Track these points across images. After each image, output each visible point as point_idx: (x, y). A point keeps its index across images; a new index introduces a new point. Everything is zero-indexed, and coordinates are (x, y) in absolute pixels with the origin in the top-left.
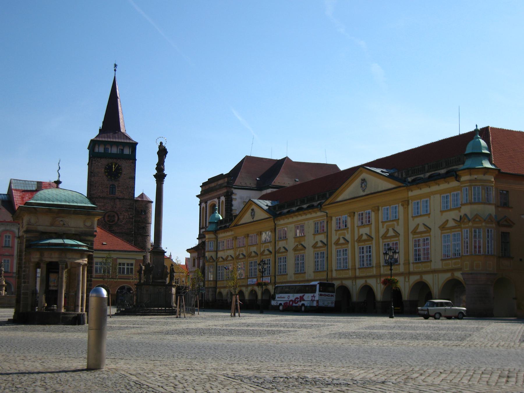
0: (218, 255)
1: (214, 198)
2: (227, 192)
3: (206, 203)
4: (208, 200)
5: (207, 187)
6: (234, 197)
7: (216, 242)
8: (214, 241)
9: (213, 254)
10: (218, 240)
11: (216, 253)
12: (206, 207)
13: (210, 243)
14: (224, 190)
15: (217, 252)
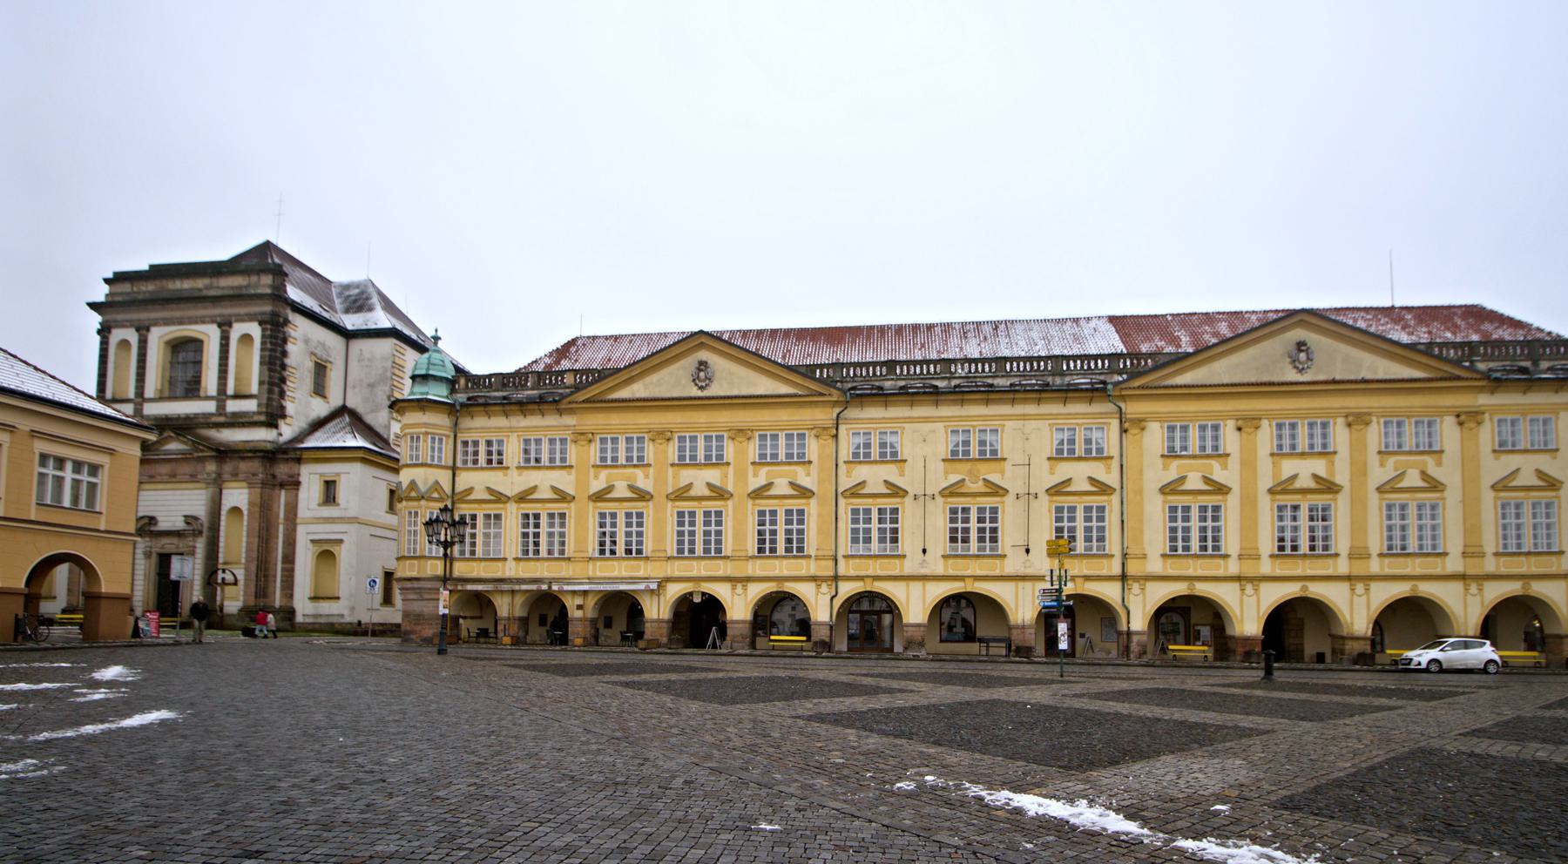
0: (457, 479)
1: (202, 320)
2: (275, 315)
3: (143, 330)
4: (156, 324)
5: (149, 287)
6: (290, 330)
7: (451, 441)
8: (448, 436)
9: (444, 478)
10: (459, 435)
11: (450, 472)
12: (143, 344)
13: (433, 439)
14: (268, 308)
15: (454, 469)
